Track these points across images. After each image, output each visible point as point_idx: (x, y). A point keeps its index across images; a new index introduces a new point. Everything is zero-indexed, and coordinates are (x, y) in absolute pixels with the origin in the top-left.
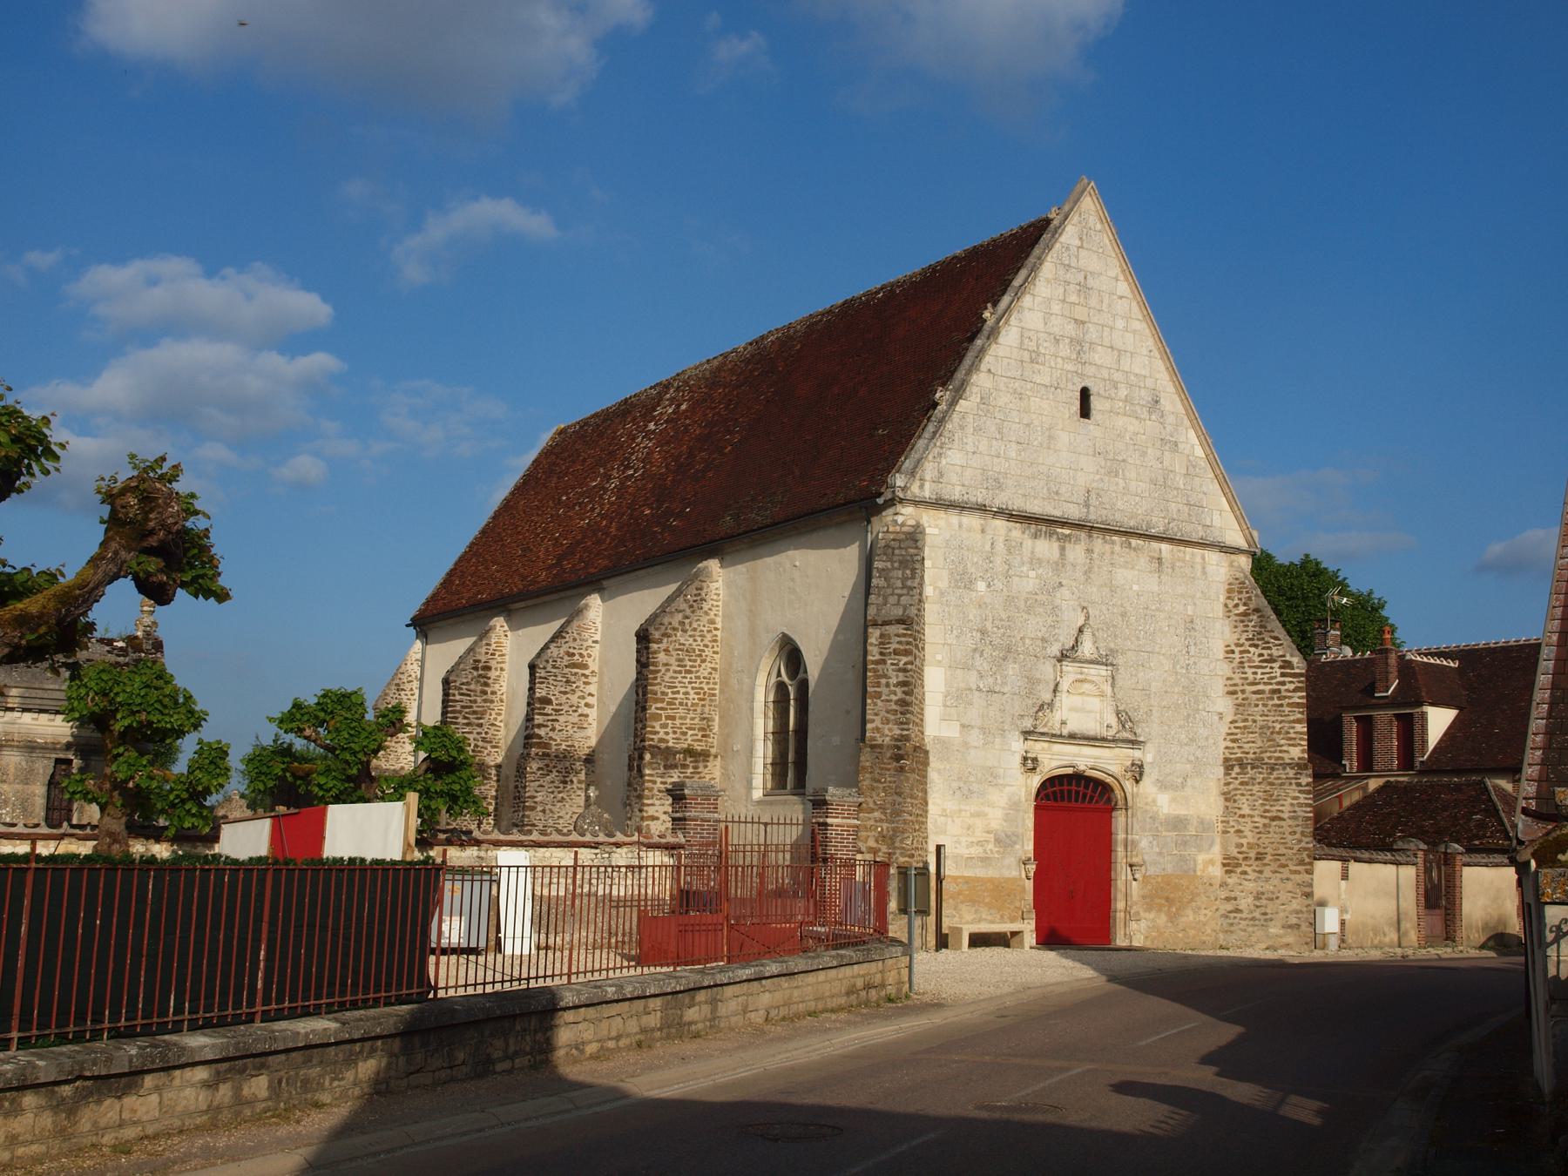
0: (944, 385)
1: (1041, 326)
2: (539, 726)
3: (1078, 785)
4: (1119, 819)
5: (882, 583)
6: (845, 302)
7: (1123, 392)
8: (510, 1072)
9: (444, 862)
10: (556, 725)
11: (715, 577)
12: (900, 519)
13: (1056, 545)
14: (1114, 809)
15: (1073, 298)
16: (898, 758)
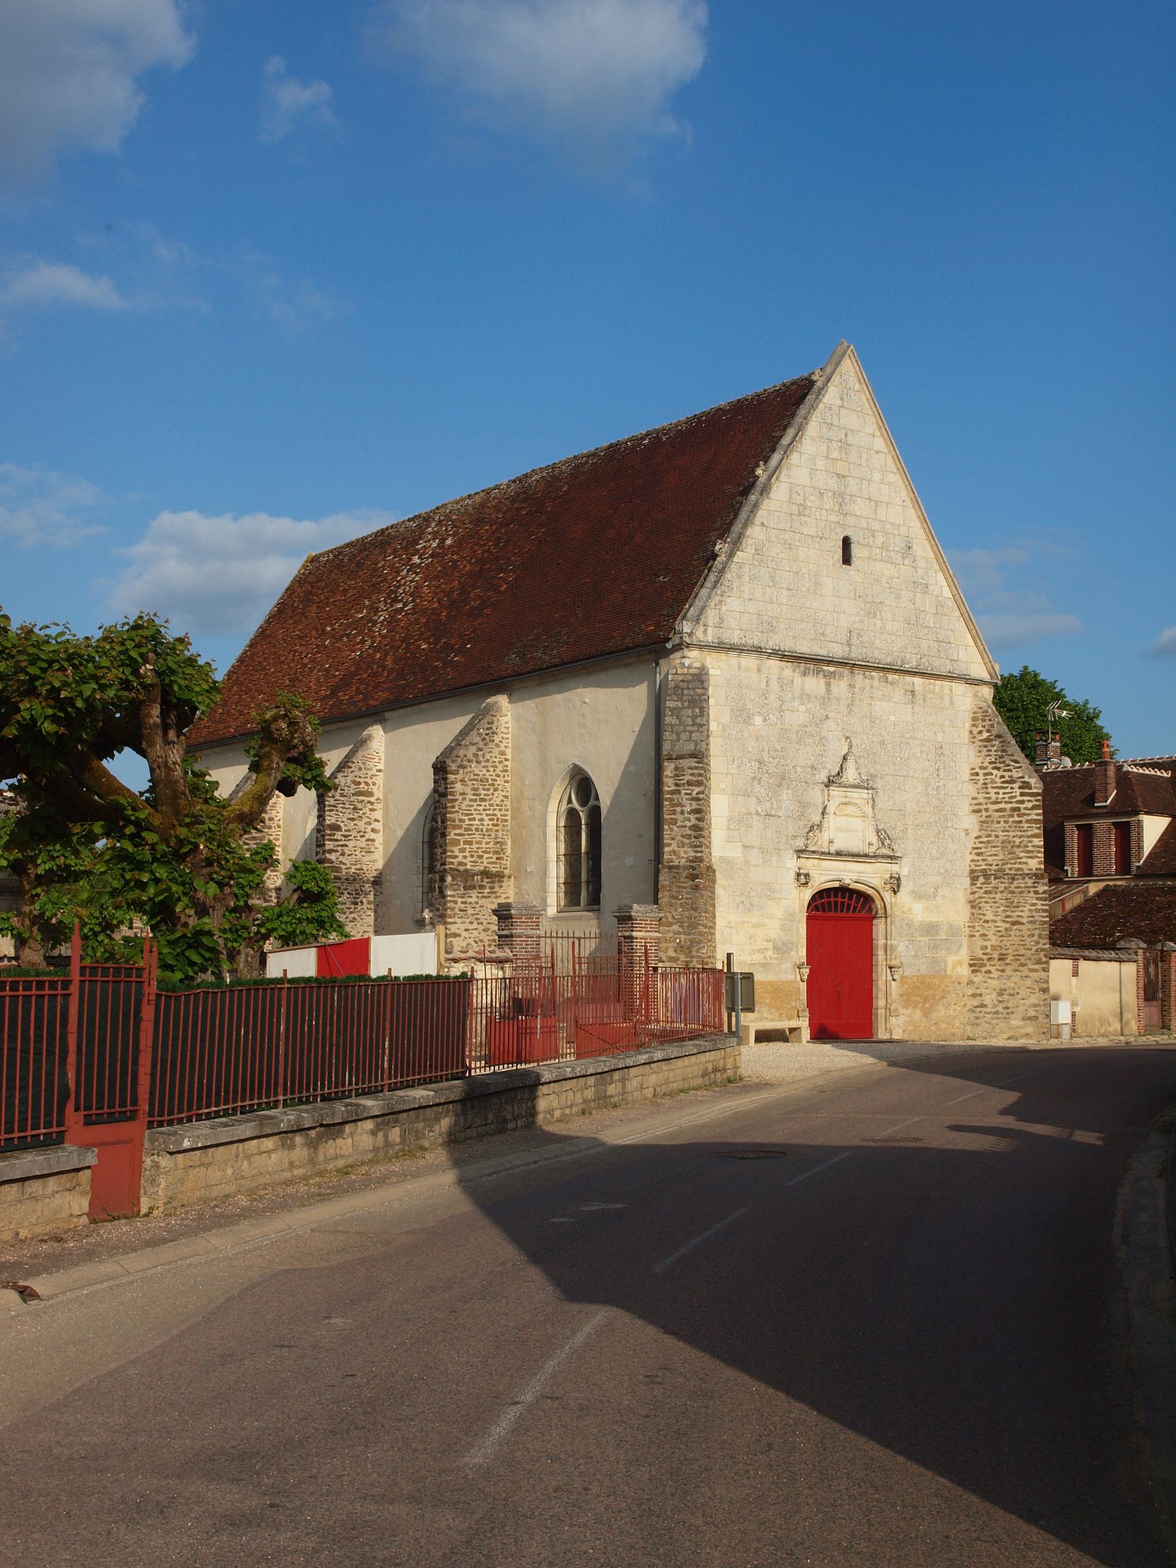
0: (721, 537)
1: (807, 482)
2: (330, 851)
3: (843, 897)
4: (879, 927)
5: (674, 721)
6: (611, 446)
7: (880, 540)
8: (515, 1129)
9: (472, 976)
10: (346, 850)
11: (504, 712)
12: (687, 662)
13: (822, 681)
14: (874, 918)
15: (835, 454)
16: (693, 877)
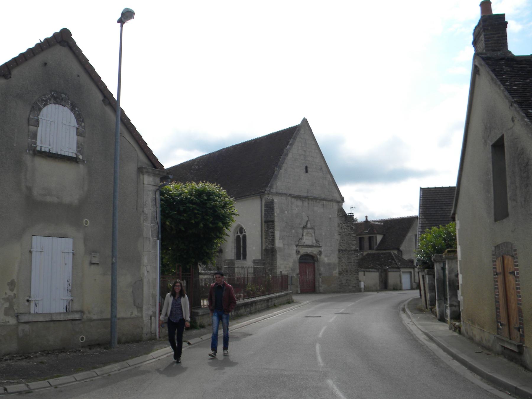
7: (314, 166)
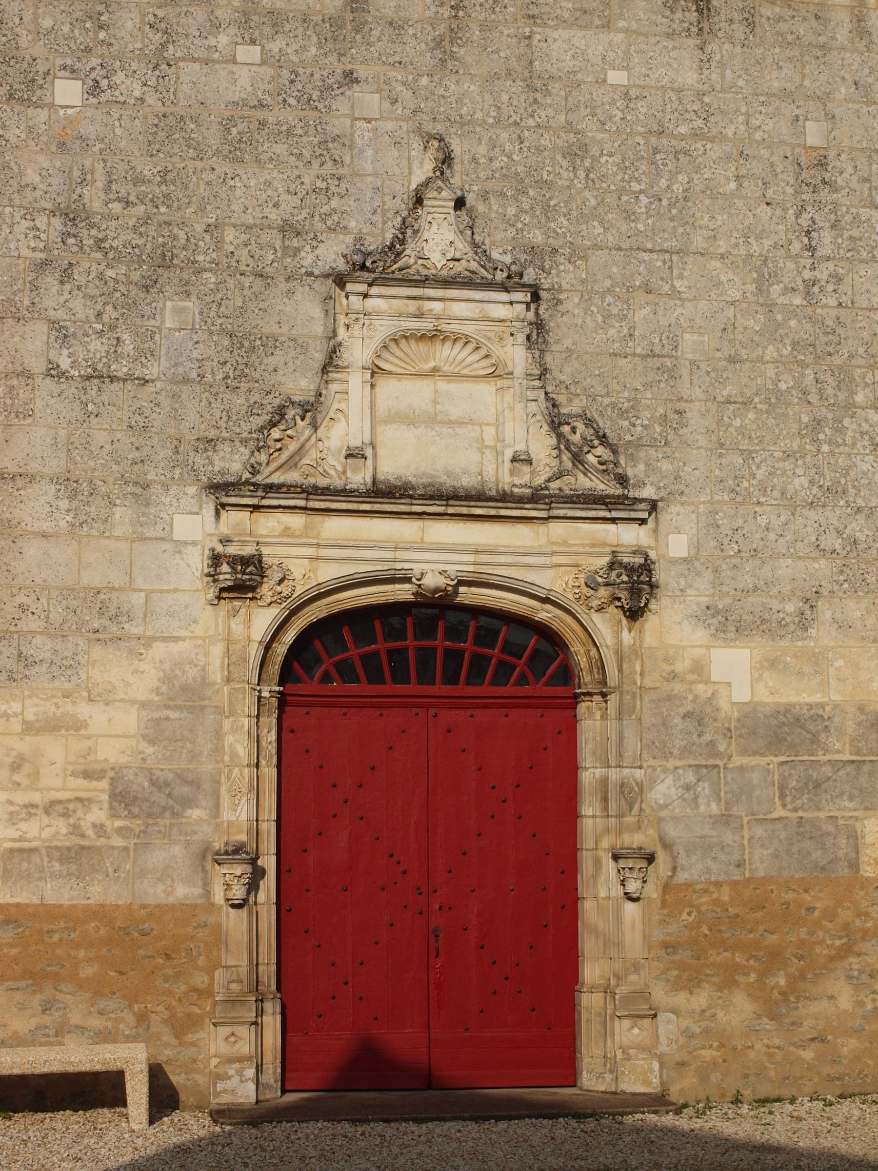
4: (592, 724)
